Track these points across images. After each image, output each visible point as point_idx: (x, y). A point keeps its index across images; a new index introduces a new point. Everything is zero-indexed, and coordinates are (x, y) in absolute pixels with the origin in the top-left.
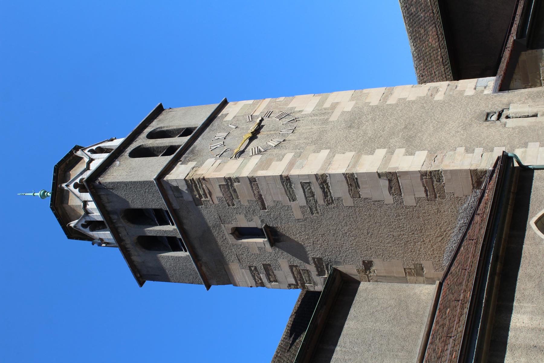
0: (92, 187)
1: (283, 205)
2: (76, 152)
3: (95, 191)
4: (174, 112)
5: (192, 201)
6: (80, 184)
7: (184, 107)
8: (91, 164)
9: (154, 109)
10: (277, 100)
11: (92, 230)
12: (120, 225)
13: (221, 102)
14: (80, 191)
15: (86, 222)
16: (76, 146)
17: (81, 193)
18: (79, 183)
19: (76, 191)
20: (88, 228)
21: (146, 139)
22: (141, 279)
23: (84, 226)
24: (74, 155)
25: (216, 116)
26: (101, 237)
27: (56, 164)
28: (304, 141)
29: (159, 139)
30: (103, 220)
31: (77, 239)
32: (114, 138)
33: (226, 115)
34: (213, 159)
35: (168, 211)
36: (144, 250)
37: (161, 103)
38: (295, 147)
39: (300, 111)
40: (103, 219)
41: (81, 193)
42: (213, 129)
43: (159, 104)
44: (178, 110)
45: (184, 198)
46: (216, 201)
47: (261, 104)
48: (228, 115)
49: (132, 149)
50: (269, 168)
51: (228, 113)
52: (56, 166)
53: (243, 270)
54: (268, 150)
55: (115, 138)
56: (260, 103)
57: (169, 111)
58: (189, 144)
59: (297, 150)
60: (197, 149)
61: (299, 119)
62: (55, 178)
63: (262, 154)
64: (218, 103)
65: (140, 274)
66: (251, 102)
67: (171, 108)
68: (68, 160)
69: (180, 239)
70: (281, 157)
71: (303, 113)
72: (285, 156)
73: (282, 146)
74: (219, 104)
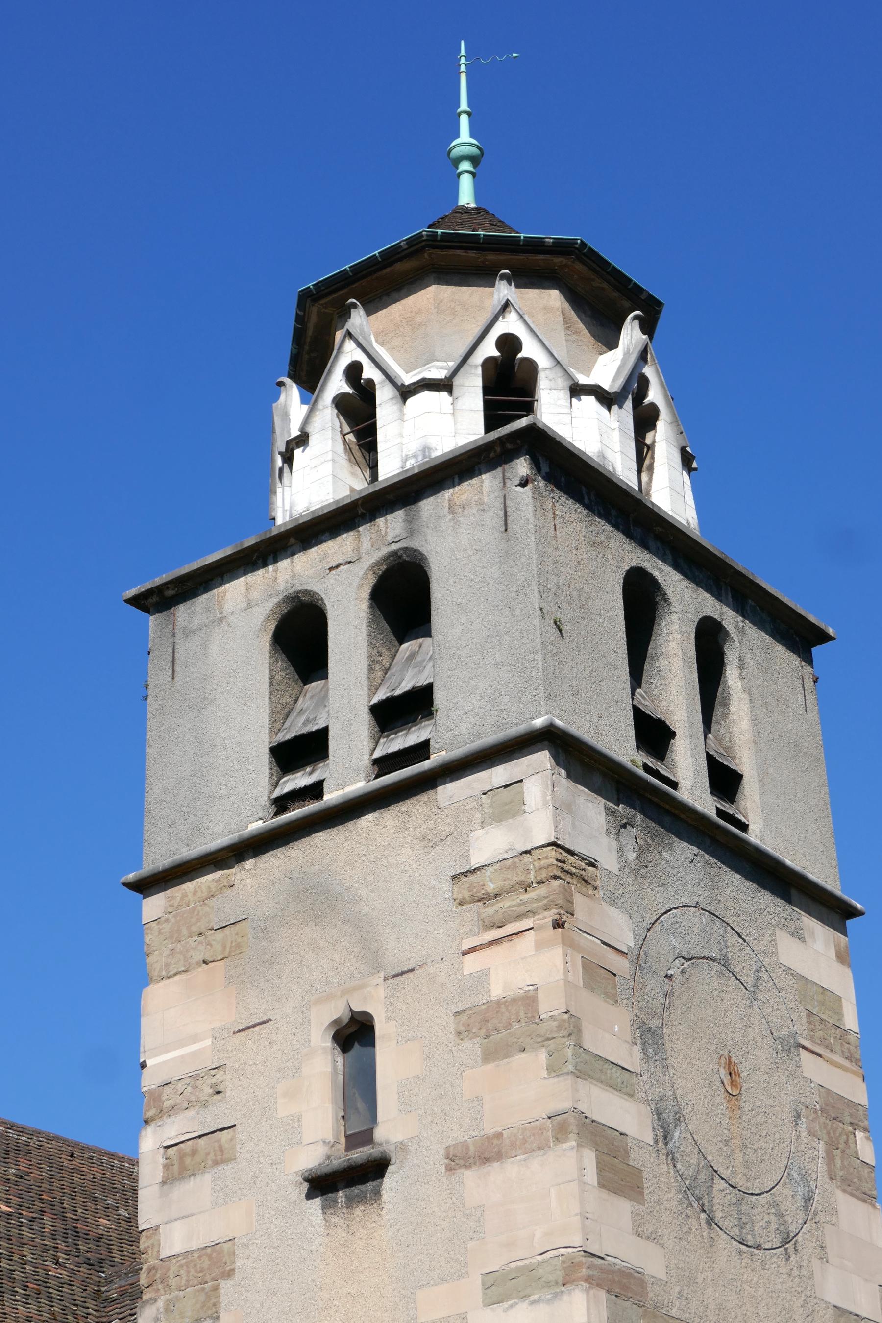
0: (509, 446)
1: (470, 1245)
2: (636, 318)
3: (492, 455)
4: (801, 698)
5: (468, 862)
6: (517, 362)
7: (823, 740)
8: (592, 398)
9: (812, 619)
10: (859, 1135)
11: (340, 402)
12: (366, 544)
13: (846, 897)
14: (488, 363)
15: (370, 382)
16: (660, 304)
17: (480, 368)
18: (520, 356)
19: (489, 349)
20: (347, 389)
21: (697, 620)
22: (154, 599)
23: (354, 372)
24: (627, 304)
25: (794, 892)
26: (312, 440)
27: (589, 244)
28: (712, 1307)
29: (696, 675)
30: (380, 479)
31: (299, 319)
32: (695, 465)
33: (798, 935)
34: (631, 936)
35: (428, 758)
36: (272, 627)
37: (833, 639)
38: (687, 1274)
39: (823, 1248)
40: (386, 479)
41: (479, 371)
42: (741, 896)
43: (831, 631)
44: (810, 714)
45: (480, 832)
46: (472, 964)
47: (845, 1069)
48: (798, 941)
49: (656, 573)
50: (604, 1194)
51: (802, 939)
52: (583, 244)
53: (208, 1042)
54: (671, 1166)
55: (696, 469)
56: (846, 1063)
57: (806, 677)
58: (682, 816)
59: (677, 1289)
60: (665, 854)
61: (793, 1258)
62: (535, 246)
63: (656, 1142)
64: (842, 891)
65: (173, 597)
66: (851, 1021)
67: (815, 682)
68: (605, 285)
69: (315, 791)
70: (649, 1228)
71: (816, 1264)
72: (651, 1245)
73: (688, 1216)
74: (838, 892)
